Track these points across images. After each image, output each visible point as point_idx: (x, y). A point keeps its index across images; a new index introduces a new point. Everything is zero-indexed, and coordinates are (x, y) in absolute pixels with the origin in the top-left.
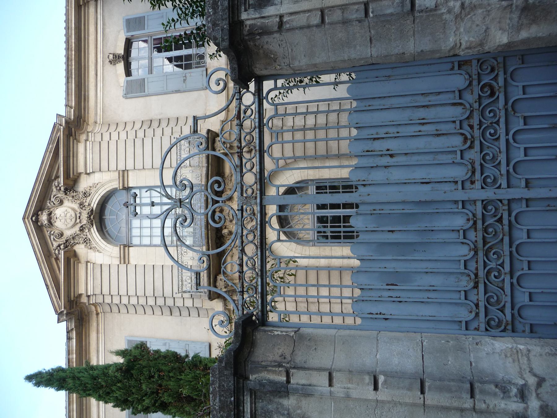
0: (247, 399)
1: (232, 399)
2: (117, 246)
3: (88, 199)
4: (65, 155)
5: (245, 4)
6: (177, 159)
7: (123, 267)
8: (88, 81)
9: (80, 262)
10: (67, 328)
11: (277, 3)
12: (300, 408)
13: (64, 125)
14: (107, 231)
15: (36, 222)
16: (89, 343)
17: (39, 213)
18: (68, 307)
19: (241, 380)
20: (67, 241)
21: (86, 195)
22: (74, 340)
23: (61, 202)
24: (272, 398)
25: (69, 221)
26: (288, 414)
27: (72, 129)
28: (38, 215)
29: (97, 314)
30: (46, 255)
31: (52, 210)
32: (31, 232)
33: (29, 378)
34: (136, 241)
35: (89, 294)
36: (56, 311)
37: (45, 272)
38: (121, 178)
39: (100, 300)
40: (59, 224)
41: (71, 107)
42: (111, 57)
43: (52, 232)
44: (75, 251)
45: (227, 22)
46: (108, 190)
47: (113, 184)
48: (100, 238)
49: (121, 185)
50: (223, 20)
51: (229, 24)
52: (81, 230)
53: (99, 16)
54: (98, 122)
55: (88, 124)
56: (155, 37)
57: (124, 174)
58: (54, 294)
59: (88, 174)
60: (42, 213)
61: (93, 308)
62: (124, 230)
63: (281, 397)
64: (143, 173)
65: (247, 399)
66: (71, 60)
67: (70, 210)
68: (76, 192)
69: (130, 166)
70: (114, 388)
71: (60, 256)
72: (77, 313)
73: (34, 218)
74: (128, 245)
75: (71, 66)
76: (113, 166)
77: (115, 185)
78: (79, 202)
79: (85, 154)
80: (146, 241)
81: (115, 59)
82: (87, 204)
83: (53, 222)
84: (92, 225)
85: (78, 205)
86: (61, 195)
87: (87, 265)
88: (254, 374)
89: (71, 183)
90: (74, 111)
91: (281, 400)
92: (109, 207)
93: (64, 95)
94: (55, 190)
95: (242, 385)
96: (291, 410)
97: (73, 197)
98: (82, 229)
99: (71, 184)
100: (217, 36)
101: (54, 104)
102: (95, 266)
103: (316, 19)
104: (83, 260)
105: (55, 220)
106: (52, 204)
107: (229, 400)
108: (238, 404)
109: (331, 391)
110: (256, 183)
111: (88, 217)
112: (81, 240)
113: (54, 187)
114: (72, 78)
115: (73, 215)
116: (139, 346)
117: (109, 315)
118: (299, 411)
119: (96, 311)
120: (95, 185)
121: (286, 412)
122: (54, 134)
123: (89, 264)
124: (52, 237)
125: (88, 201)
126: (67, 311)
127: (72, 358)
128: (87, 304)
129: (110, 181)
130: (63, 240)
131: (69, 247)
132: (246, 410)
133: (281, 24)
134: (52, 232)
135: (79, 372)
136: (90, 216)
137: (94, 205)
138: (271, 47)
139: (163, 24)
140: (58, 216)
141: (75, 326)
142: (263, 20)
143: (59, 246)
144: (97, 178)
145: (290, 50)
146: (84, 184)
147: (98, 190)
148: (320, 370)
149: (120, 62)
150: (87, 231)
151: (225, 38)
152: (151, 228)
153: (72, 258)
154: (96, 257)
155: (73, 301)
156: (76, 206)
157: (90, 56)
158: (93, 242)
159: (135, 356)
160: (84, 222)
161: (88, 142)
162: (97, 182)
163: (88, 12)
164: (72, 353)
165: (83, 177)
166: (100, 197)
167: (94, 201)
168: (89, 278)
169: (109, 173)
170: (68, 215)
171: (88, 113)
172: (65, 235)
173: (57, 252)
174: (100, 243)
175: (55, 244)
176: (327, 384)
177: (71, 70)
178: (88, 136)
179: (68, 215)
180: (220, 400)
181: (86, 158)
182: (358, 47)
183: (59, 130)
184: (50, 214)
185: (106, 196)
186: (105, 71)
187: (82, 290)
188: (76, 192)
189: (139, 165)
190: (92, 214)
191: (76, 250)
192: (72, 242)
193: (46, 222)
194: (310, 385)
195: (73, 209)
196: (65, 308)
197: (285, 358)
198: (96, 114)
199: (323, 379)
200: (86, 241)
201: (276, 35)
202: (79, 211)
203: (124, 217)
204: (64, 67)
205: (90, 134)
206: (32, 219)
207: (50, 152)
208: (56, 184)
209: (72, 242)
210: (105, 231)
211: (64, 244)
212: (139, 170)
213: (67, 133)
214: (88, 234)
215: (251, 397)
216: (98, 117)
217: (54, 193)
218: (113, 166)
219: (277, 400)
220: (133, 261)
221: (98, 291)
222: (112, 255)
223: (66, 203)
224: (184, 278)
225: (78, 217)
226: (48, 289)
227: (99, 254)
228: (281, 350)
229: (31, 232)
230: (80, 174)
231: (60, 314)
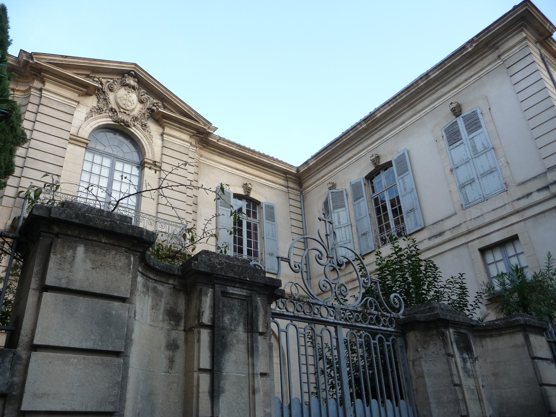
0: (244, 293)
1: (248, 279)
2: (89, 137)
3: (140, 127)
4: (183, 122)
6: (169, 221)
7: (67, 136)
8: (233, 161)
12: (238, 342)
15: (129, 73)
17: (136, 80)
18: (34, 66)
20: (104, 92)
21: (144, 126)
23: (141, 102)
24: (243, 316)
25: (124, 102)
26: (232, 330)
27: (202, 135)
28: (134, 77)
30: (95, 69)
31: (137, 91)
36: (36, 54)
37: (80, 61)
40: (122, 92)
41: (218, 141)
42: (250, 186)
44: (91, 95)
47: (150, 153)
48: (101, 124)
51: (449, 320)
53: (277, 186)
54: (201, 158)
55: (200, 149)
56: (258, 225)
57: (156, 166)
58: (55, 60)
61: (23, 88)
63: (244, 324)
65: (244, 293)
66: (252, 154)
67: (133, 107)
71: (91, 80)
73: (133, 73)
75: (248, 153)
76: (165, 159)
77: (149, 156)
78: (139, 117)
79: (180, 139)
81: (247, 189)
82: (136, 124)
84: (115, 122)
85: (136, 116)
86: (148, 105)
87: (76, 101)
88: (261, 302)
89: (157, 117)
90: (214, 142)
91: (242, 324)
93: (227, 138)
95: (255, 289)
96: (235, 333)
97: (144, 114)
101: (225, 130)
102: (73, 109)
106: (142, 94)
107: (247, 275)
108: (241, 283)
111: (124, 120)
112: (101, 105)
114: (239, 149)
115: (128, 108)
118: (235, 341)
119: (18, 90)
120: (151, 137)
121: (233, 327)
123: (76, 104)
124: (112, 81)
125: (138, 126)
126: (31, 63)
128: (31, 85)
129: (153, 152)
130: (106, 90)
131: (97, 92)
132: (235, 289)
133: (449, 355)
136: (124, 123)
137: (133, 130)
138: (431, 346)
142: (450, 343)
143: (101, 84)
144: (157, 141)
145: (430, 359)
146: (153, 128)
147: (147, 139)
149: (245, 192)
150: (110, 114)
153: (87, 90)
154: (81, 113)
155: (40, 74)
156: (135, 113)
157: (231, 162)
158: (98, 116)
160: (120, 116)
161: (189, 145)
162: (153, 139)
163: (281, 178)
165: (160, 130)
167: (136, 131)
169: (159, 153)
170: (129, 104)
171: (209, 152)
172: (109, 93)
173: (96, 79)
175: (104, 81)
177: (245, 151)
178: (194, 146)
179: (129, 104)
180: (235, 265)
181: (177, 138)
182: (437, 410)
183: (205, 125)
184: (134, 88)
185: (140, 145)
186: (239, 177)
187: (48, 86)
190: (125, 125)
192: (101, 97)
193: (128, 82)
195: (133, 110)
196: (36, 63)
198: (207, 159)
200: (99, 110)
201: (443, 351)
204: (247, 146)
207: (188, 111)
208: (160, 105)
209: (101, 97)
211: (102, 89)
213: (201, 130)
214: (107, 114)
215: (244, 296)
216: (204, 160)
217: (151, 99)
219: (242, 320)
220: (70, 147)
222: (81, 130)
223: (139, 106)
225: (125, 111)
226: (62, 56)
227: (84, 117)
231: (31, 56)
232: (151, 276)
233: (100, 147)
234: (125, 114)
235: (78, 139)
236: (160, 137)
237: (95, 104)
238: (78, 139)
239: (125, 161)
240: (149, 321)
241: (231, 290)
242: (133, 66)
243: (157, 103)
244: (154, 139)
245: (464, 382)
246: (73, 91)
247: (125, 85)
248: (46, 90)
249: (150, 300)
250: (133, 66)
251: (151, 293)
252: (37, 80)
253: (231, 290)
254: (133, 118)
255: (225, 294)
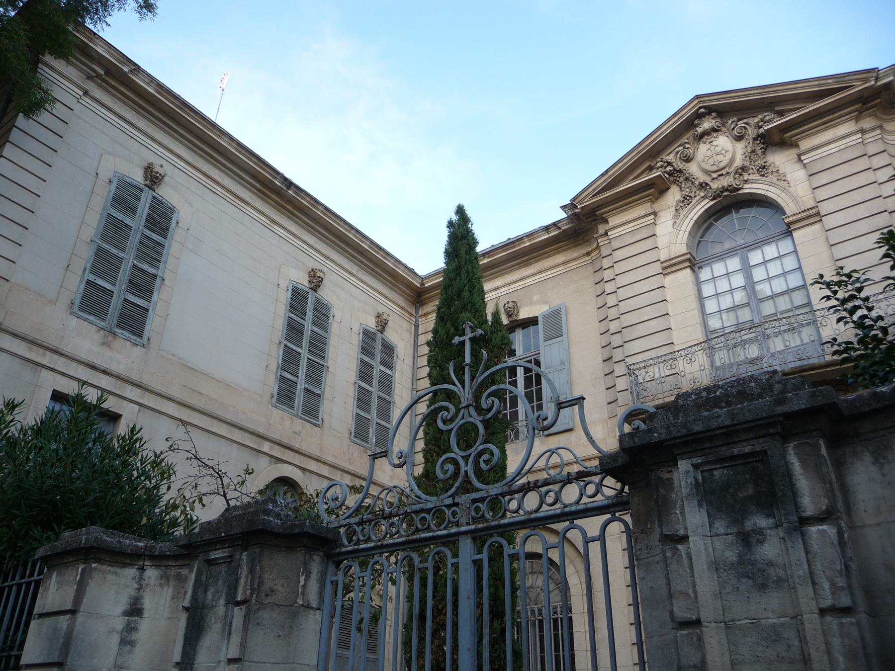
3: (756, 177)
4: (821, 110)
5: (708, 463)
7: (657, 268)
9: (653, 202)
10: (559, 221)
11: (716, 525)
13: (879, 83)
14: (711, 225)
15: (698, 116)
16: (550, 256)
19: (240, 543)
20: (680, 171)
21: (763, 170)
22: (547, 236)
23: (739, 138)
25: (711, 161)
28: (709, 113)
29: (588, 254)
30: (651, 152)
31: (724, 129)
32: (679, 116)
33: (460, 211)
34: (705, 274)
35: (609, 233)
37: (625, 161)
38: (804, 214)
39: (605, 251)
40: (703, 150)
43: (687, 146)
44: (668, 189)
45: (664, 437)
46: (779, 200)
47: (791, 204)
49: (791, 219)
50: (668, 428)
52: (701, 184)
57: (813, 216)
58: (598, 187)
59: (800, 160)
60: (714, 118)
61: (595, 245)
62: (718, 249)
64: (823, 248)
67: (729, 156)
68: (764, 153)
69: (829, 222)
70: (449, 324)
72: (582, 225)
73: (702, 110)
74: (693, 264)
76: (823, 194)
77: (790, 208)
78: (747, 164)
80: (708, 290)
82: (746, 177)
83: (704, 140)
84: (712, 200)
86: (752, 132)
87: (649, 214)
91: (224, 595)
92: (752, 213)
94: (757, 120)
97: (753, 151)
98: (703, 186)
99: (775, 140)
100: (656, 420)
103: (681, 611)
104: (657, 206)
105: (708, 142)
106: (733, 126)
109: (220, 662)
110: (565, 506)
111: (723, 187)
113: (760, 117)
115: (722, 165)
116: (506, 341)
117: (590, 269)
120: (782, 178)
122: (854, 77)
123: (652, 217)
124: (681, 148)
125: (752, 177)
127: (524, 243)
128: (595, 236)
129: (794, 199)
131: (671, 179)
134: (687, 146)
135: (468, 272)
136: (727, 190)
137: (747, 189)
139: (821, 276)
140: (715, 143)
141: (564, 231)
143: (670, 164)
144: (796, 175)
146: (781, 160)
148: (243, 645)
150: (702, 194)
151: (636, 440)
152: (731, 290)
153: (656, 190)
156: (738, 162)
158: (686, 210)
159: (491, 340)
160: (715, 185)
164: (530, 240)
165: (792, 153)
166: (763, 192)
167: (756, 187)
168: (632, 225)
169: (809, 191)
170: (720, 157)
172: (688, 165)
173: (659, 165)
174: (688, 220)
175: (670, 158)
176: (230, 656)
178: (873, 129)
179: (720, 157)
183: (866, 80)
187: (613, 221)
188: (764, 153)
189: (835, 236)
191: (671, 190)
193: (700, 130)
194: (230, 633)
195: (732, 160)
197: (267, 595)
199: (234, 653)
200: (686, 200)
202: (733, 169)
203: (740, 242)
205: (878, 131)
206: (701, 108)
207: (819, 85)
208: (767, 118)
209: (681, 179)
210: (711, 220)
211: (675, 170)
212: (827, 238)
214: (698, 198)
218: (823, 194)
219: (225, 590)
220: (669, 281)
221: (616, 244)
223: (740, 147)
224: (650, 369)
225: (720, 173)
226: (603, 175)
227: (670, 226)
228: (280, 588)
229: (679, 116)
230: (797, 146)
231: (572, 205)
232: (170, 563)
233: (718, 249)
234: (721, 178)
235: (673, 261)
236: (798, 166)
237: (678, 197)
238: (673, 261)
239: (758, 244)
240: (166, 614)
241: (213, 555)
242: (696, 101)
243: (762, 120)
244: (789, 178)
245: (708, 610)
246: (642, 203)
247: (700, 137)
248: (611, 229)
249: (171, 590)
250: (696, 101)
251: (172, 583)
252: (599, 223)
253: (213, 555)
254: (736, 173)
255: (210, 562)
